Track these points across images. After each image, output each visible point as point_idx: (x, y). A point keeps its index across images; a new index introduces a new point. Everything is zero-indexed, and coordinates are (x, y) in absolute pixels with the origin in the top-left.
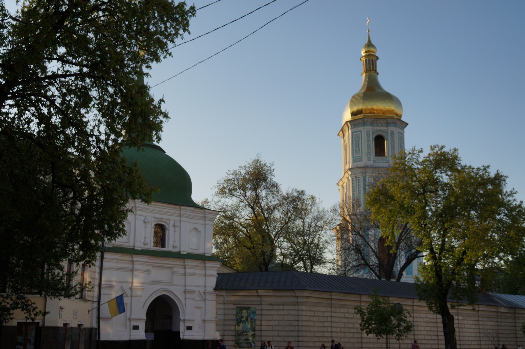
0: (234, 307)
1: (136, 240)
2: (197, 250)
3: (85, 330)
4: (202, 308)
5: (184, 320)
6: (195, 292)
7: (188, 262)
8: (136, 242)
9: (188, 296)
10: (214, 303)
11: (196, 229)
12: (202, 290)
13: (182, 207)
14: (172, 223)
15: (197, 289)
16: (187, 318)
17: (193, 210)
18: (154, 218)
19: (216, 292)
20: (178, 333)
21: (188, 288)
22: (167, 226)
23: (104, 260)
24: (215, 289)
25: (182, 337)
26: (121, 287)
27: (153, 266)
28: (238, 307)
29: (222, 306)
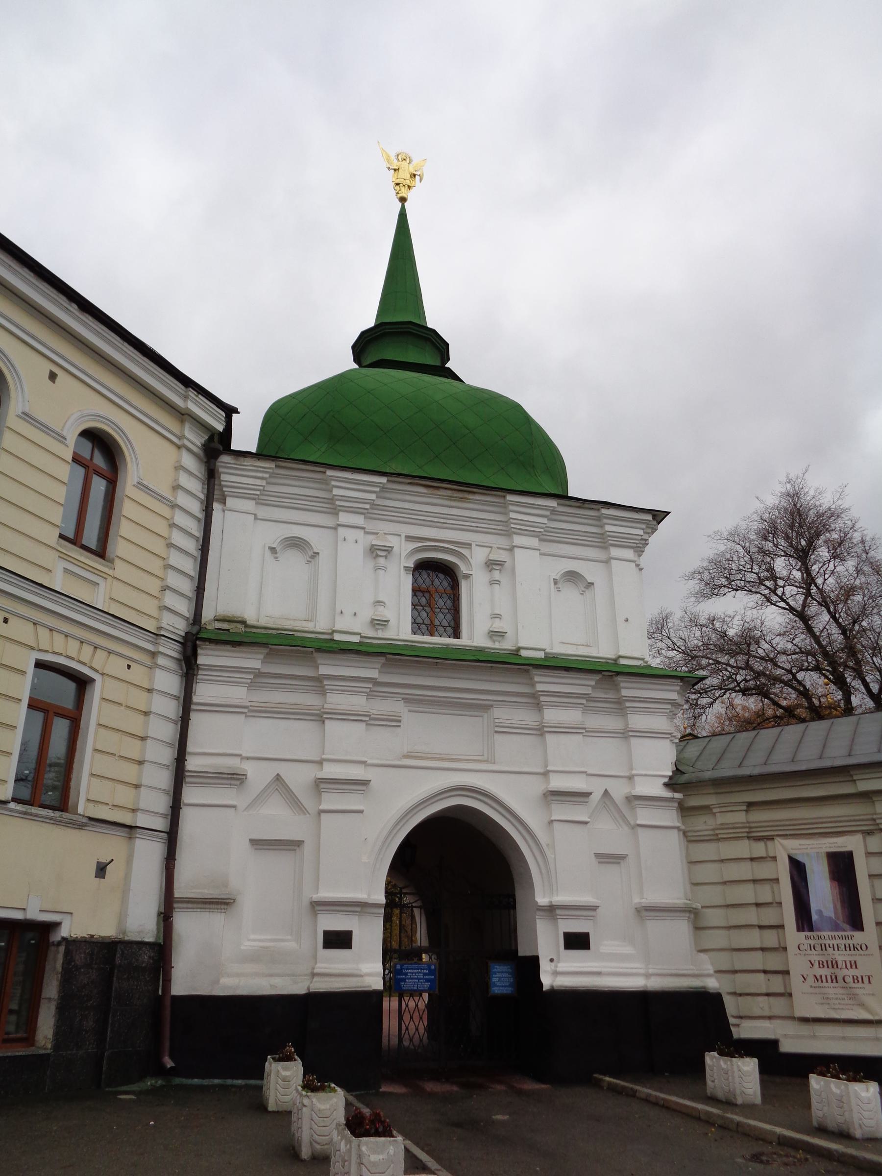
1: (338, 611)
2: (587, 646)
3: (62, 949)
5: (551, 910)
7: (544, 683)
8: (338, 618)
9: (561, 811)
10: (674, 838)
11: (572, 577)
12: (619, 791)
13: (510, 498)
14: (478, 556)
15: (596, 788)
17: (553, 511)
18: (409, 538)
19: (678, 795)
20: (533, 963)
21: (558, 783)
22: (463, 568)
23: (201, 675)
24: (671, 785)
25: (547, 980)
26: (278, 777)
27: (407, 700)
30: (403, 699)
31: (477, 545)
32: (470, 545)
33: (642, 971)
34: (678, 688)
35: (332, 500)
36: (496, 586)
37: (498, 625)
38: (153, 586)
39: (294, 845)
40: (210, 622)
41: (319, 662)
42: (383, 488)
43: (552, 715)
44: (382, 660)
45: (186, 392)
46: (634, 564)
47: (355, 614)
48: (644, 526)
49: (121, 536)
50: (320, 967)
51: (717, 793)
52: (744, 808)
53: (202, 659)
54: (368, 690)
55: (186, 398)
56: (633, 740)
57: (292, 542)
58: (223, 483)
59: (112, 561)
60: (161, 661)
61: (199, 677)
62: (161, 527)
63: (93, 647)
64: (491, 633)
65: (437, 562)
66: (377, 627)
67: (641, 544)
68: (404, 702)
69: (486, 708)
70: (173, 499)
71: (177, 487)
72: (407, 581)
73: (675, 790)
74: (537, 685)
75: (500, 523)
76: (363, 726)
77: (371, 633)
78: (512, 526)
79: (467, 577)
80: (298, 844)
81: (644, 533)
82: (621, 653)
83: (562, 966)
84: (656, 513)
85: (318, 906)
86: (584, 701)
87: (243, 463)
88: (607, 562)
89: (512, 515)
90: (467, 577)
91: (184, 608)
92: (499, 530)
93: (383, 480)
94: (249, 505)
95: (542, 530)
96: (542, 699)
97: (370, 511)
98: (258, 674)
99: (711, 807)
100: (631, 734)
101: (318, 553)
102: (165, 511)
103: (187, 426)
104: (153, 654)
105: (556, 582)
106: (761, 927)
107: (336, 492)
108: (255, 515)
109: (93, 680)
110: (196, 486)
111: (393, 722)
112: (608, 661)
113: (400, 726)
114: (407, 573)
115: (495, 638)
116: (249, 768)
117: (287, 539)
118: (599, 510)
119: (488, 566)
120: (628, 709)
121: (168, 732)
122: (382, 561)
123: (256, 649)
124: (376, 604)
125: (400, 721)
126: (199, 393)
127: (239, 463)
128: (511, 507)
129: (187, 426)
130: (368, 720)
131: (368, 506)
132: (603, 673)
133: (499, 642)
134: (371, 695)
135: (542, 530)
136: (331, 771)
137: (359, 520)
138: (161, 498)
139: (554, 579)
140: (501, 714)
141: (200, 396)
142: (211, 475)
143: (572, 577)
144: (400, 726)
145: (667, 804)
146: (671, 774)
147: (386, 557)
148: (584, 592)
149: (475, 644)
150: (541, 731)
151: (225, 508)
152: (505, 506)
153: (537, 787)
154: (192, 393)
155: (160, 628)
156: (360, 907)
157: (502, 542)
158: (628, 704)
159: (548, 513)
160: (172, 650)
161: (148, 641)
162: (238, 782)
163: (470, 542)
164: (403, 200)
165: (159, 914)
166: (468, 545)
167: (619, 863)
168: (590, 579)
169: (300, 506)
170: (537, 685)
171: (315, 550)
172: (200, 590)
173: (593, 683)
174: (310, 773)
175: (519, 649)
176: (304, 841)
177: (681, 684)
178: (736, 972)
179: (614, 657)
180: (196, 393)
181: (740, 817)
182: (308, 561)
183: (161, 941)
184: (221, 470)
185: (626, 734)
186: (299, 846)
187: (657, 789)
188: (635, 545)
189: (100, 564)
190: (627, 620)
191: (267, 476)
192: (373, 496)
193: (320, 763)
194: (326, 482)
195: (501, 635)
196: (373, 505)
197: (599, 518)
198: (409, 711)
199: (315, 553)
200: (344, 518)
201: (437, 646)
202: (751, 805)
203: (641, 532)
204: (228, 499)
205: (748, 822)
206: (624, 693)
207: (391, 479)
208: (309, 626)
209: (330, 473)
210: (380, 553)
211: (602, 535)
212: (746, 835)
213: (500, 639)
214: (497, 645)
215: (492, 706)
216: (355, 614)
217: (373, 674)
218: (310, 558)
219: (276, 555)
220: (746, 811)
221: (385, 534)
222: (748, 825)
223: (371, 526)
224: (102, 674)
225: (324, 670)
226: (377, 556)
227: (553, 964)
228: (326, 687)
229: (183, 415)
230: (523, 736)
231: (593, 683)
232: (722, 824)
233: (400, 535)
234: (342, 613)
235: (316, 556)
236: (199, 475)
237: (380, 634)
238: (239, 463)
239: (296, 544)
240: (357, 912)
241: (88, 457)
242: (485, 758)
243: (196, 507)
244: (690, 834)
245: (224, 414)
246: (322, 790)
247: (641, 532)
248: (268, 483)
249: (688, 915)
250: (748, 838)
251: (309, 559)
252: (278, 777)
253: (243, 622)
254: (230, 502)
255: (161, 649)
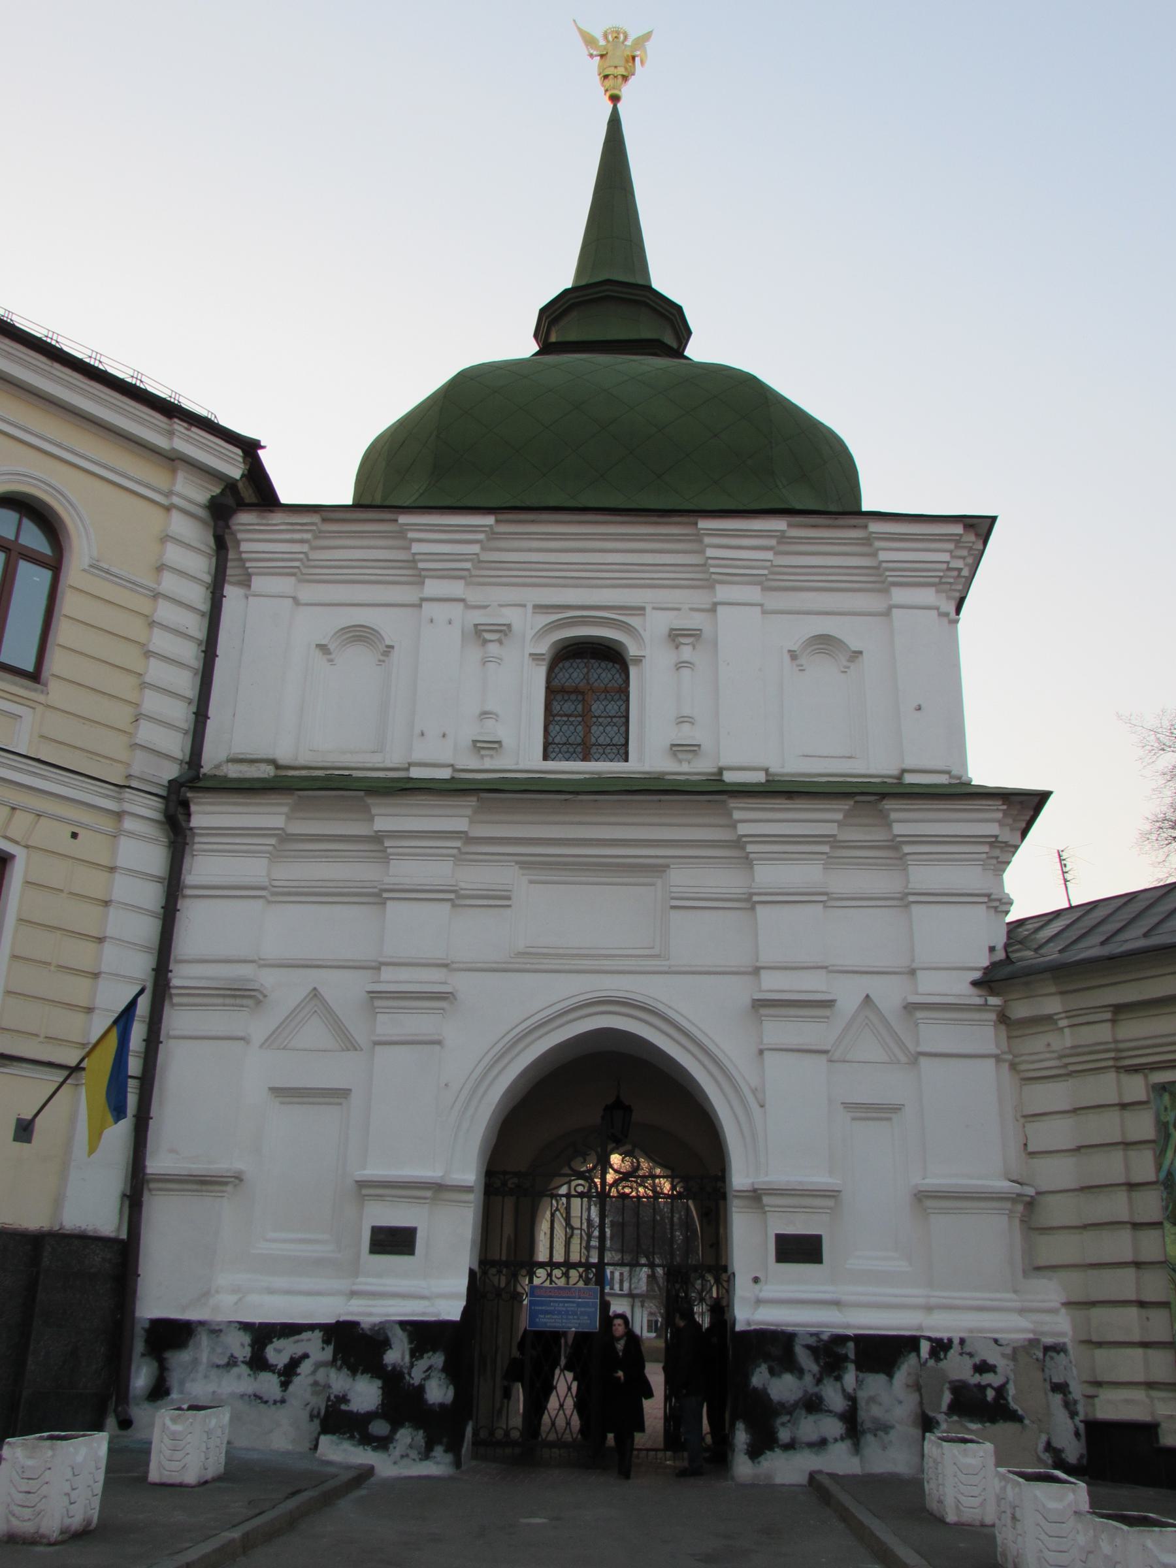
0: (1136, 1088)
4: (897, 1109)
5: (755, 1196)
6: (829, 1004)
9: (778, 1031)
11: (824, 643)
13: (704, 524)
14: (655, 625)
15: (847, 992)
16: (778, 1174)
17: (782, 538)
18: (540, 608)
19: (994, 1001)
21: (774, 984)
22: (633, 650)
23: (200, 843)
26: (315, 994)
27: (526, 865)
28: (1162, 1088)
29: (1056, 1095)
30: (517, 863)
31: (654, 608)
32: (643, 609)
33: (921, 1301)
34: (1000, 815)
35: (413, 562)
36: (686, 672)
37: (686, 734)
38: (120, 716)
39: (339, 1095)
40: (218, 766)
41: (374, 811)
42: (492, 535)
43: (768, 875)
44: (472, 801)
45: (170, 425)
46: (934, 613)
47: (444, 736)
48: (951, 546)
49: (60, 645)
50: (365, 1283)
51: (1061, 993)
52: (1108, 1016)
53: (197, 821)
54: (455, 851)
55: (171, 434)
56: (914, 908)
57: (351, 634)
58: (244, 556)
59: (46, 685)
60: (129, 824)
61: (196, 847)
62: (136, 629)
63: (8, 808)
64: (674, 749)
65: (593, 643)
66: (483, 752)
67: (950, 577)
68: (521, 868)
69: (658, 869)
70: (155, 586)
71: (161, 568)
72: (538, 677)
73: (993, 992)
74: (739, 826)
75: (690, 569)
76: (447, 906)
77: (472, 762)
78: (712, 570)
79: (638, 660)
80: (344, 1093)
81: (952, 557)
82: (909, 763)
83: (768, 1291)
84: (975, 521)
85: (368, 1189)
86: (826, 848)
87: (270, 522)
88: (887, 613)
89: (710, 552)
90: (638, 660)
91: (176, 745)
92: (693, 579)
93: (490, 520)
94: (284, 585)
95: (765, 572)
96: (750, 848)
97: (474, 572)
98: (285, 837)
99: (1055, 1017)
100: (911, 898)
101: (392, 647)
102: (142, 604)
103: (181, 476)
104: (119, 815)
105: (793, 656)
106: (1136, 1226)
107: (416, 548)
108: (294, 598)
109: (12, 857)
110: (200, 565)
111: (499, 899)
112: (885, 780)
113: (509, 906)
114: (537, 665)
115: (681, 756)
116: (267, 979)
117: (344, 630)
118: (866, 527)
119: (674, 641)
120: (909, 857)
121: (147, 929)
122: (493, 648)
123: (274, 798)
124: (482, 717)
125: (509, 898)
126: (191, 424)
127: (264, 522)
128: (707, 540)
129: (181, 476)
130: (455, 898)
131: (468, 565)
132: (859, 798)
133: (689, 763)
134: (460, 858)
135: (765, 572)
136: (391, 979)
137: (456, 588)
138: (133, 585)
139: (789, 651)
140: (682, 878)
141: (194, 429)
142: (222, 545)
143: (824, 643)
144: (509, 906)
145: (976, 1016)
146: (986, 963)
147: (500, 642)
148: (848, 667)
149: (647, 768)
150: (749, 902)
151: (248, 593)
152: (698, 538)
153: (741, 992)
154: (179, 426)
155: (129, 776)
156: (438, 1190)
157: (701, 598)
158: (907, 849)
159: (773, 542)
160: (150, 808)
161: (106, 797)
162: (250, 1002)
163: (643, 604)
164: (615, 99)
165: (124, 1195)
166: (640, 610)
167: (889, 1119)
168: (855, 645)
169: (367, 577)
170: (739, 826)
171: (388, 642)
172: (201, 715)
173: (839, 816)
174: (359, 984)
175: (720, 771)
176: (350, 1090)
177: (1005, 807)
178: (1093, 1304)
179: (895, 772)
180: (185, 425)
181: (1102, 1033)
182: (380, 661)
183: (124, 1235)
184: (240, 536)
185: (905, 900)
186: (346, 1098)
187: (959, 988)
188: (937, 580)
189: (22, 687)
190: (919, 708)
191: (308, 536)
192: (476, 548)
193: (377, 967)
194: (401, 534)
195: (693, 749)
196: (478, 562)
197: (868, 541)
198: (531, 882)
199: (388, 647)
200: (433, 587)
201: (582, 776)
202: (1119, 1010)
203: (945, 557)
204: (254, 579)
205: (1116, 1041)
206: (898, 829)
207: (501, 517)
208: (375, 760)
209: (403, 519)
210: (488, 636)
211: (877, 569)
212: (1111, 1063)
213: (690, 756)
214: (685, 768)
215: (668, 866)
216: (444, 736)
217: (461, 824)
218: (382, 655)
219: (329, 657)
220: (1113, 1021)
221: (501, 606)
222: (1112, 1046)
223: (475, 595)
224: (27, 847)
225: (382, 823)
226: (485, 642)
227: (757, 1287)
228: (389, 850)
229: (173, 460)
230: (721, 912)
231: (839, 816)
232: (1073, 1047)
233: (524, 606)
234: (423, 734)
235: (389, 652)
236: (203, 547)
237: (488, 764)
238: (264, 522)
239: (360, 635)
240: (425, 1198)
241: (13, 538)
242: (656, 951)
243: (198, 596)
244: (1023, 1067)
245: (239, 452)
246: (377, 1010)
247: (945, 557)
248: (313, 548)
249: (1008, 1205)
250: (1118, 1069)
251: (382, 658)
252: (315, 994)
253: (273, 762)
254: (258, 583)
255: (127, 807)
